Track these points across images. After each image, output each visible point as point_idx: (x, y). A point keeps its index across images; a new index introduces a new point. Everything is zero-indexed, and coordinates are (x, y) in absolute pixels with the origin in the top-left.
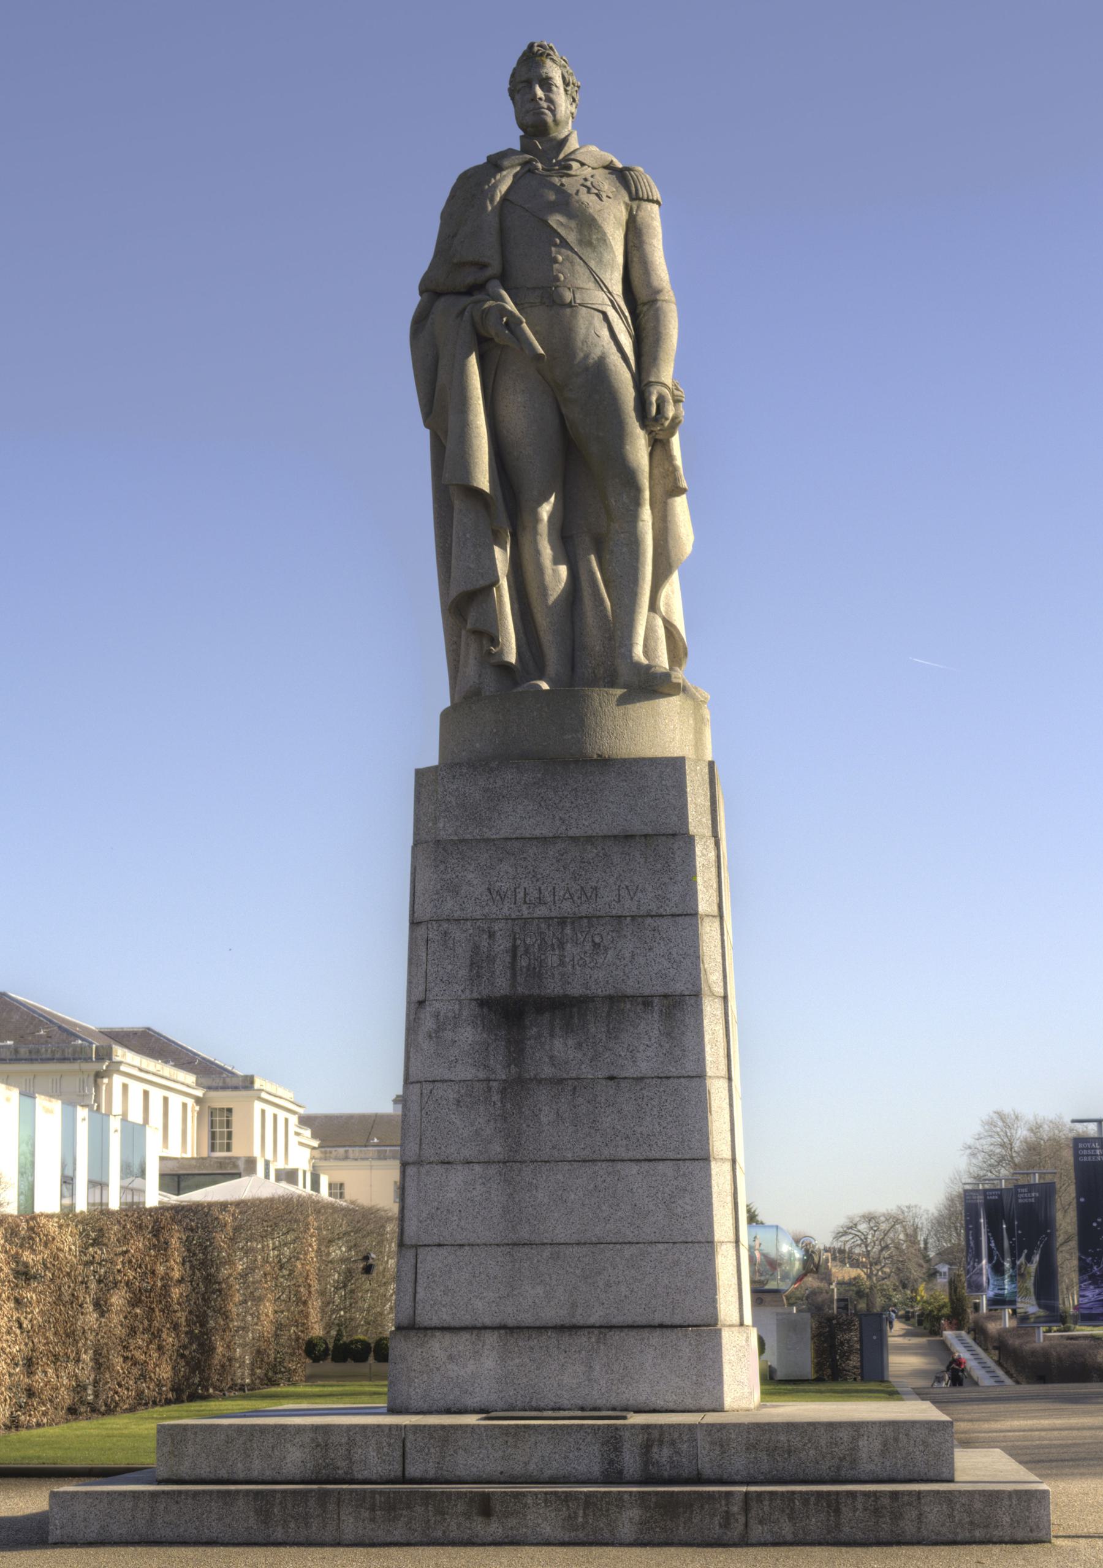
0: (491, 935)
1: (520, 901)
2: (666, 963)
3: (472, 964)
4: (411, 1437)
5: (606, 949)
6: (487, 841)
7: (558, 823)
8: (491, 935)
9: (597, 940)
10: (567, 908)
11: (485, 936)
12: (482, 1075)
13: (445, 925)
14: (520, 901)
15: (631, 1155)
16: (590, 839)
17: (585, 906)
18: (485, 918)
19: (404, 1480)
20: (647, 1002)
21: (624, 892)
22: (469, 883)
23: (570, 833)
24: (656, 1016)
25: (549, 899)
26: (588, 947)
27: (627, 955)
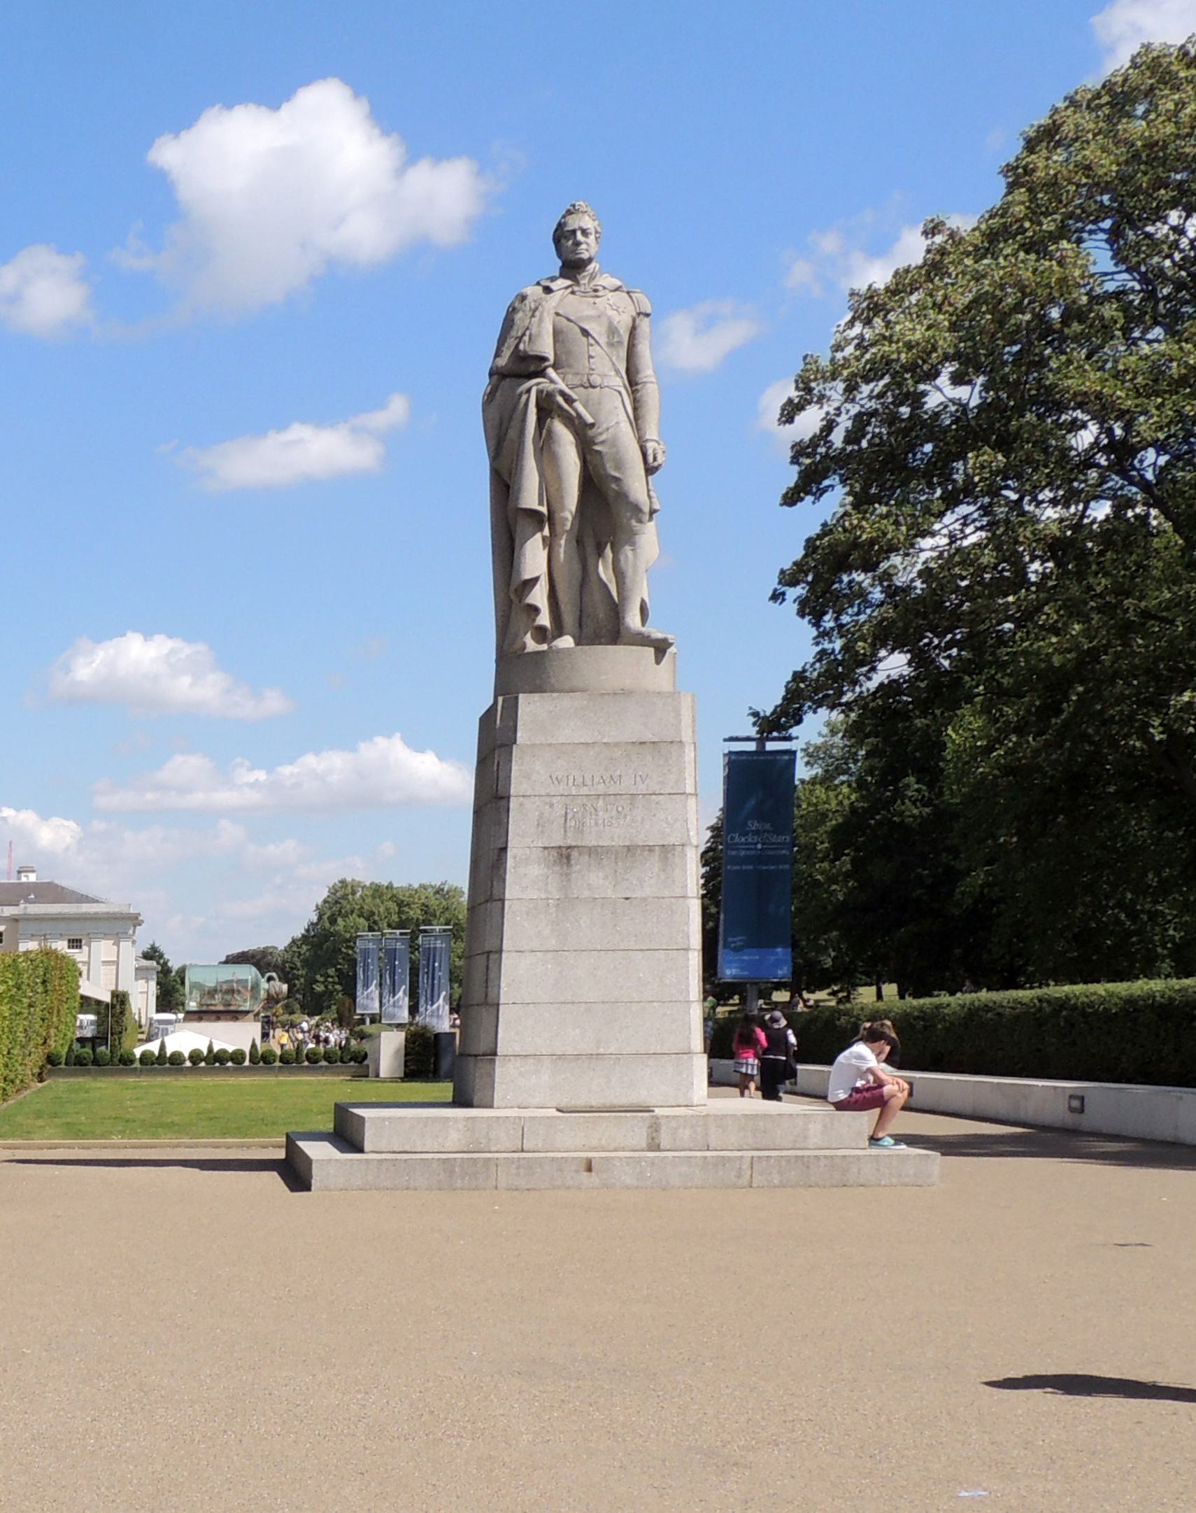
0: (551, 806)
1: (571, 784)
2: (665, 825)
3: (538, 825)
4: (527, 1124)
5: (625, 817)
6: (550, 745)
7: (596, 733)
8: (551, 806)
9: (620, 809)
10: (601, 789)
11: (547, 807)
12: (543, 896)
13: (521, 799)
14: (571, 784)
15: (637, 948)
16: (617, 744)
17: (612, 788)
18: (548, 795)
19: (522, 1151)
20: (651, 849)
21: (638, 779)
22: (538, 773)
23: (604, 741)
24: (656, 858)
25: (589, 783)
26: (614, 813)
27: (639, 819)
